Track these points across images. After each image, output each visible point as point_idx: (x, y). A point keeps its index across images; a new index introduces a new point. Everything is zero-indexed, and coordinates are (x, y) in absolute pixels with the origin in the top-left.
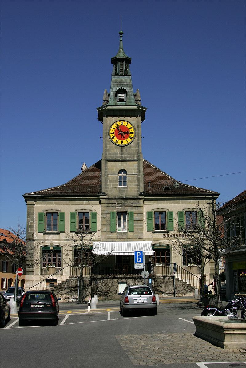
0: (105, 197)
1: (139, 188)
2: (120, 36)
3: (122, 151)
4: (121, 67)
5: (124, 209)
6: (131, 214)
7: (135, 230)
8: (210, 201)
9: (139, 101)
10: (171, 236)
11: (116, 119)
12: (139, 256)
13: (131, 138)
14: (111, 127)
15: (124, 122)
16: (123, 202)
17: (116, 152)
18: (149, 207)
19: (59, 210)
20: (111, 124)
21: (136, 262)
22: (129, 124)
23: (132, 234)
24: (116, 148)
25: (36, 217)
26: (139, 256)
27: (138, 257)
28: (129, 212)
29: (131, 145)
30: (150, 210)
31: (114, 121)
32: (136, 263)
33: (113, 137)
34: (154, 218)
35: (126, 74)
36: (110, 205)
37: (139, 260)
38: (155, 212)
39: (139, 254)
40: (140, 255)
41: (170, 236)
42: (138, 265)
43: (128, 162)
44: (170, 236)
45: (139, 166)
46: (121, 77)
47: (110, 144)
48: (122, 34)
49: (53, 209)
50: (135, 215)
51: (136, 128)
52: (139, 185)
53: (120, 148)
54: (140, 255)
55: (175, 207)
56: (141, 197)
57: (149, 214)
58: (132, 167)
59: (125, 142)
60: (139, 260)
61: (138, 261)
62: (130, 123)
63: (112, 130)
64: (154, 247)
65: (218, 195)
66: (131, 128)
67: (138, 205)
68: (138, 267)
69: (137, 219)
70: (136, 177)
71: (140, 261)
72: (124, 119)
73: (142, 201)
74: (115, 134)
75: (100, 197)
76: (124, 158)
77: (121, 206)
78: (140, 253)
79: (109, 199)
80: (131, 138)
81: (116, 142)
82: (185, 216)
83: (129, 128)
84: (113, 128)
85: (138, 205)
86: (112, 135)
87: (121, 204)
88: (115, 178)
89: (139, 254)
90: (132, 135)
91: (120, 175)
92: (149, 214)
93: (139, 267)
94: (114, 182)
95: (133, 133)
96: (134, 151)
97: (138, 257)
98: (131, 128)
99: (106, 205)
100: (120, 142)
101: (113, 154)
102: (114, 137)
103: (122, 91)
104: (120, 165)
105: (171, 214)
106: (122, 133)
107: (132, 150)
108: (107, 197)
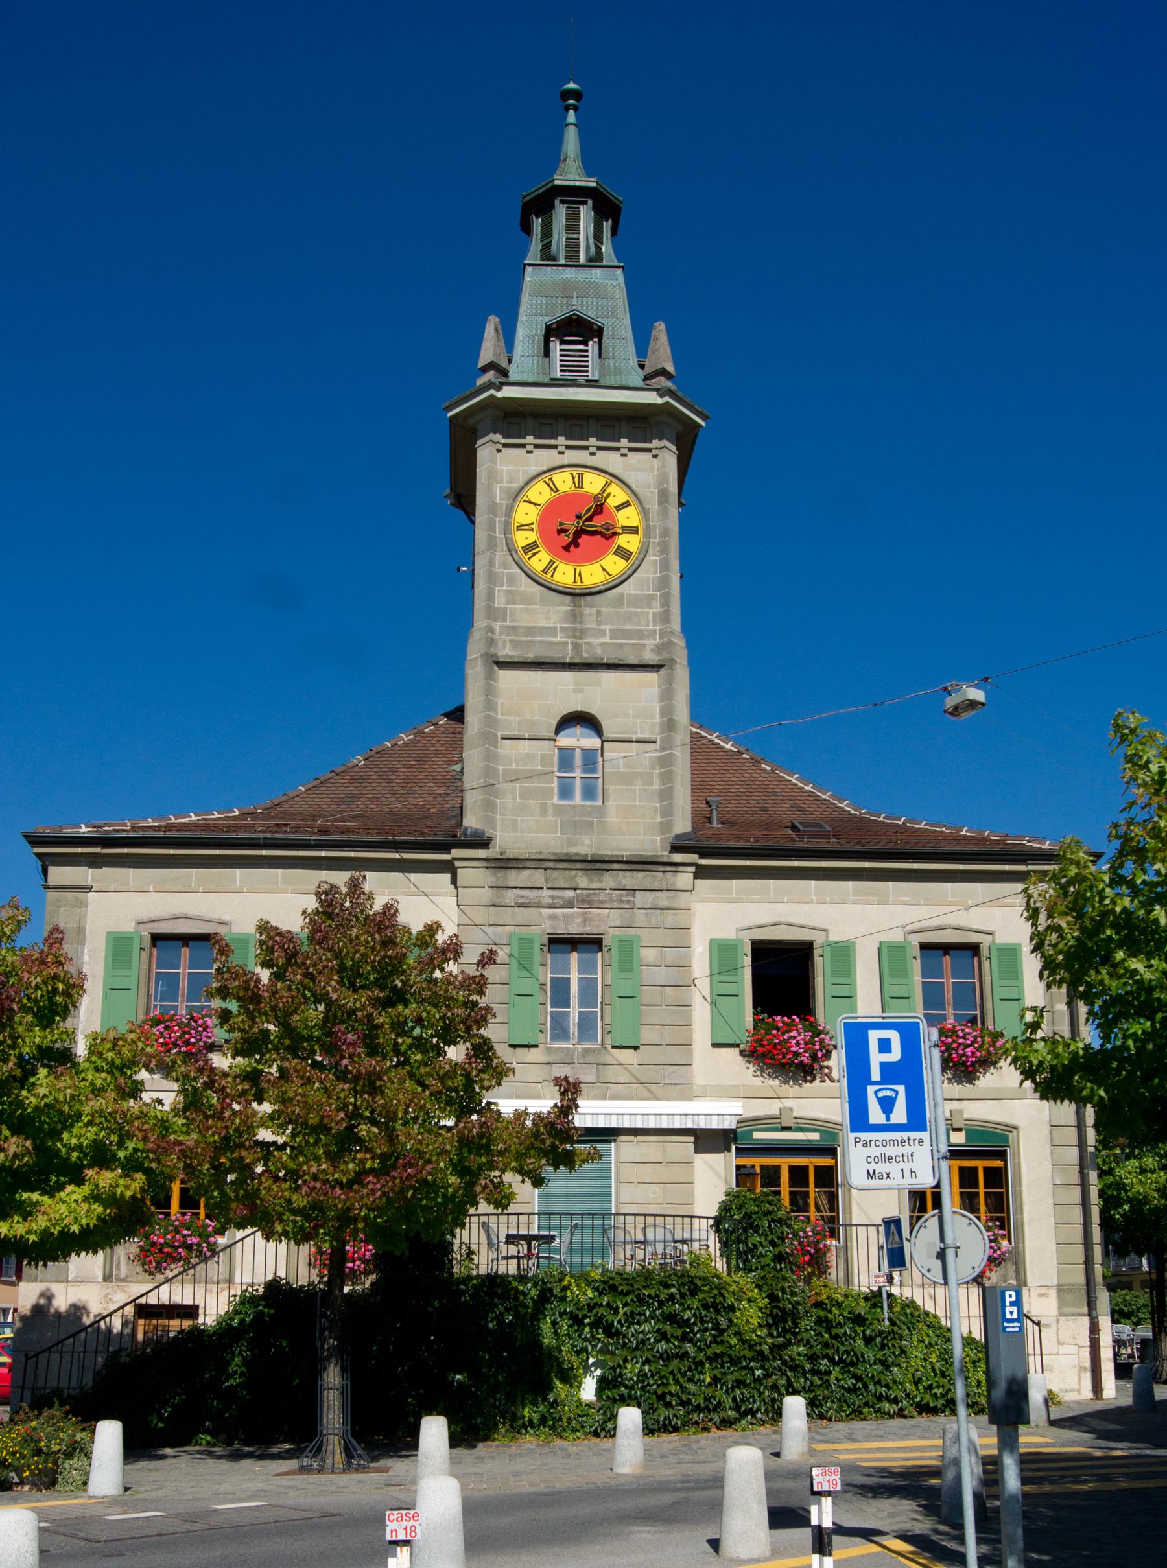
0: (481, 853)
1: (667, 812)
3: (575, 617)
4: (572, 226)
6: (628, 948)
11: (544, 458)
12: (884, 1066)
13: (623, 553)
14: (517, 495)
16: (582, 881)
17: (543, 623)
19: (226, 918)
20: (521, 482)
23: (626, 1056)
24: (544, 602)
25: (90, 957)
26: (884, 1066)
27: (876, 1075)
28: (611, 937)
29: (628, 589)
32: (865, 1136)
33: (531, 548)
36: (510, 896)
37: (887, 1105)
39: (885, 1046)
40: (895, 1055)
42: (873, 1151)
43: (607, 677)
45: (667, 695)
46: (570, 274)
47: (512, 580)
48: (577, 95)
50: (648, 955)
51: (653, 506)
52: (666, 795)
53: (564, 606)
54: (895, 1055)
56: (678, 857)
59: (592, 575)
60: (887, 1105)
61: (876, 1115)
63: (526, 514)
64: (751, 1132)
67: (663, 899)
68: (881, 1168)
69: (661, 975)
70: (651, 753)
71: (900, 1115)
73: (684, 879)
74: (542, 532)
75: (456, 853)
76: (586, 657)
77: (569, 905)
78: (894, 1036)
79: (503, 864)
80: (623, 553)
81: (545, 571)
82: (916, 967)
84: (530, 502)
85: (664, 903)
86: (522, 539)
87: (571, 894)
89: (885, 1046)
90: (630, 542)
95: (633, 530)
96: (643, 622)
97: (876, 1075)
99: (486, 895)
100: (564, 574)
101: (531, 631)
104: (564, 691)
105: (844, 952)
106: (582, 528)
107: (629, 618)
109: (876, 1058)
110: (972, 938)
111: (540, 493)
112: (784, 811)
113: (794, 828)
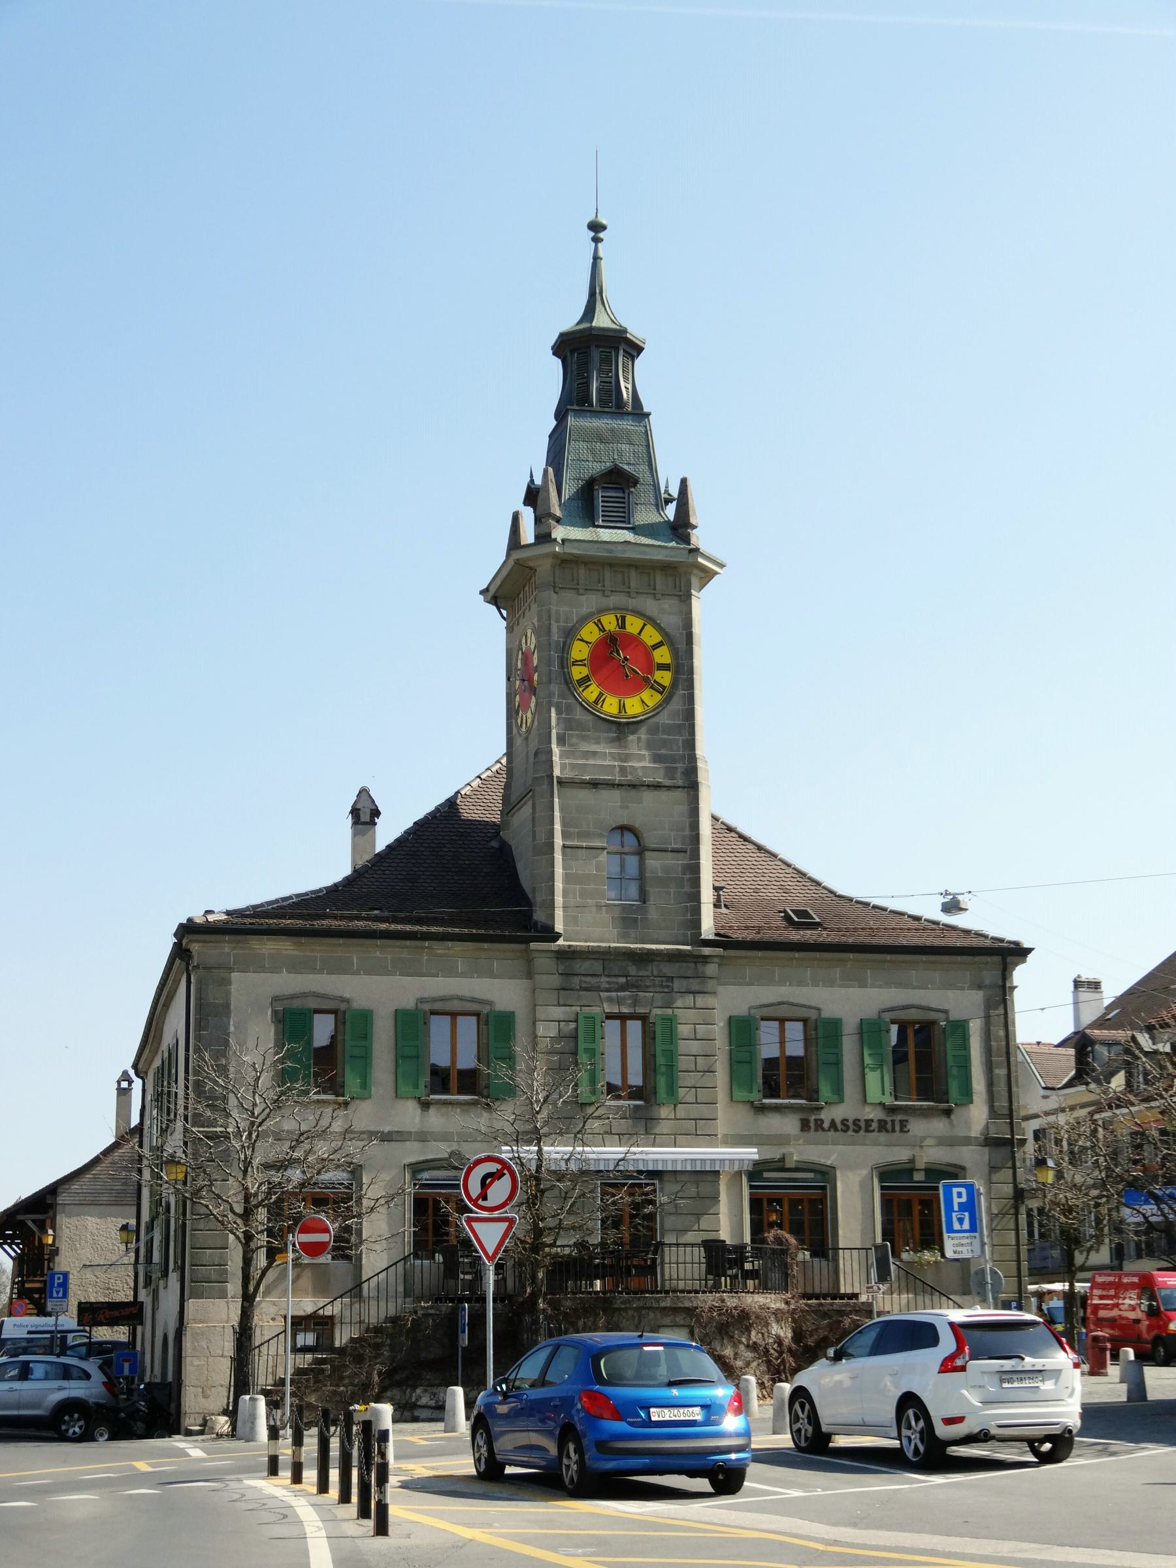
12: (959, 1204)
16: (632, 970)
19: (347, 995)
21: (950, 1230)
25: (236, 1028)
26: (959, 1204)
27: (956, 1208)
31: (585, 610)
32: (952, 1235)
33: (584, 681)
36: (576, 981)
40: (964, 1199)
41: (826, 1125)
42: (956, 1242)
44: (826, 1125)
50: (684, 1030)
54: (964, 1199)
61: (956, 1226)
64: (761, 1172)
68: (959, 1249)
69: (694, 1047)
71: (966, 1226)
72: (632, 603)
75: (533, 945)
77: (622, 988)
78: (963, 1190)
81: (596, 702)
84: (587, 643)
85: (696, 987)
86: (578, 673)
87: (623, 980)
89: (960, 1195)
90: (664, 678)
96: (675, 748)
97: (956, 1208)
100: (611, 706)
109: (956, 1201)
110: (932, 1016)
111: (590, 633)
112: (771, 893)
113: (787, 918)
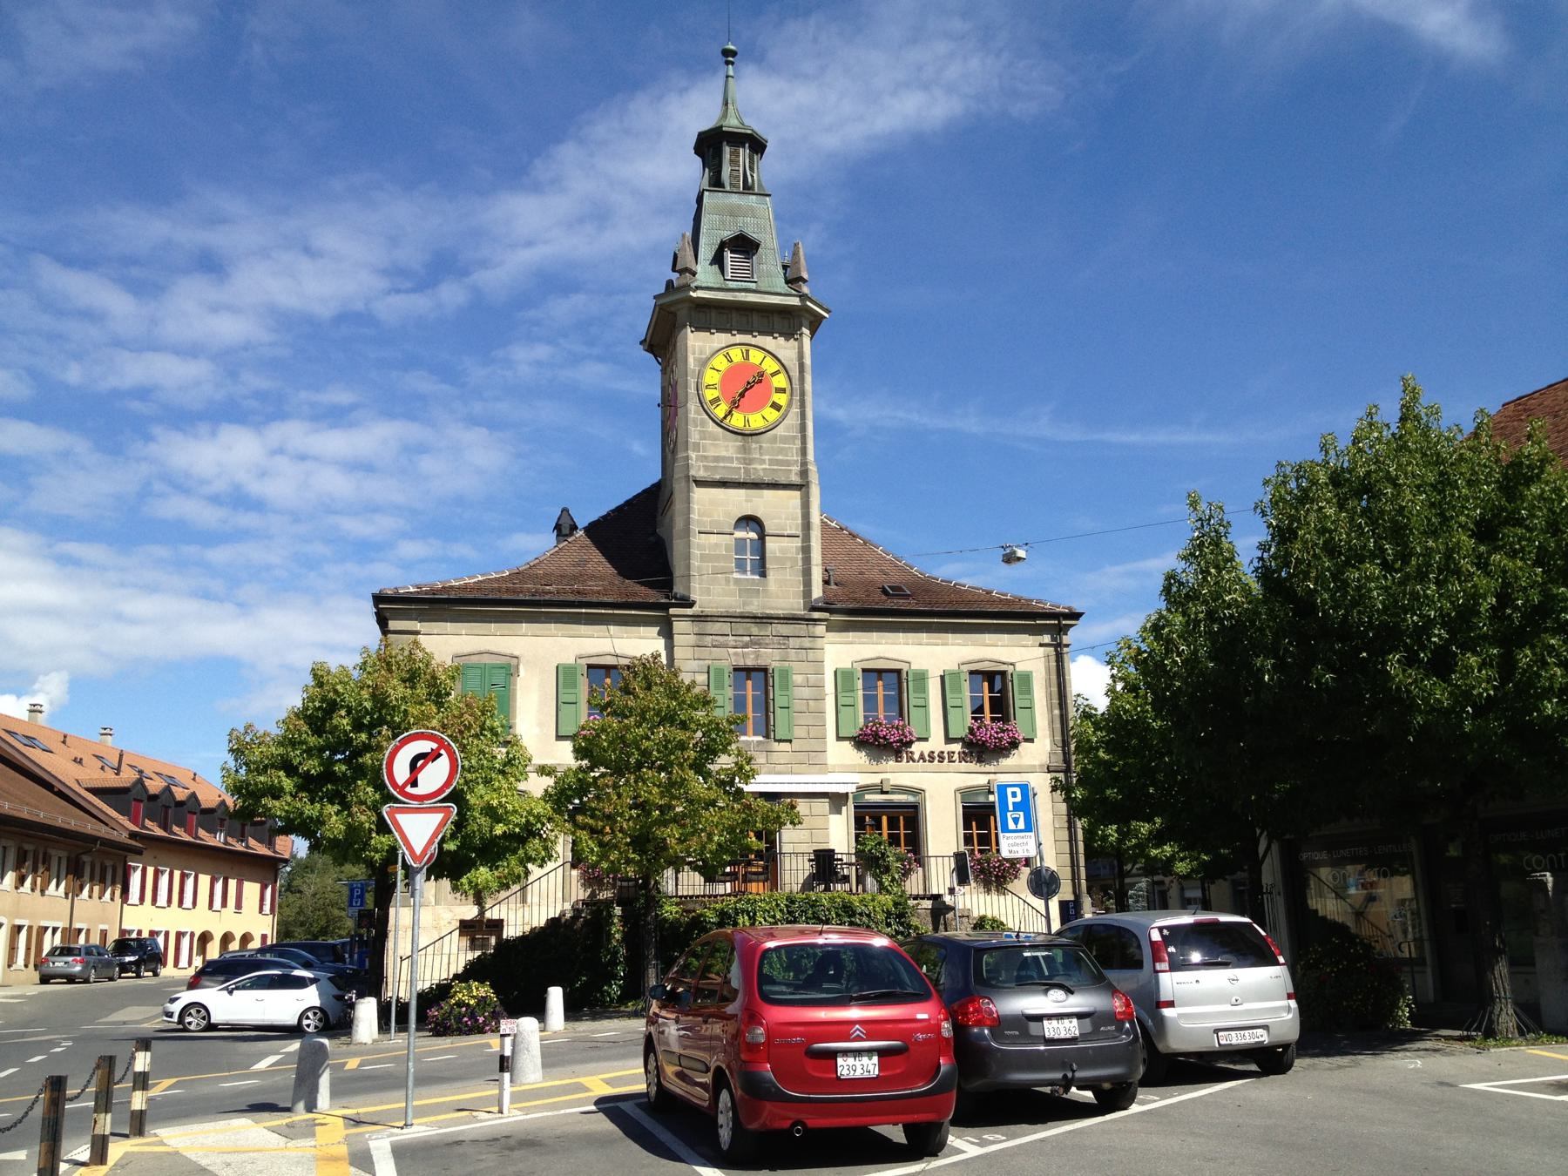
0: (689, 611)
1: (807, 584)
2: (727, 63)
3: (745, 449)
4: (734, 162)
5: (757, 657)
6: (785, 674)
7: (799, 732)
8: (1047, 639)
9: (805, 281)
10: (922, 757)
11: (722, 339)
13: (776, 407)
14: (704, 363)
15: (753, 352)
16: (755, 630)
17: (724, 454)
18: (845, 651)
20: (708, 353)
21: (1006, 829)
22: (769, 360)
23: (785, 746)
24: (725, 439)
28: (773, 664)
29: (780, 431)
30: (846, 664)
31: (717, 346)
33: (715, 401)
34: (860, 693)
35: (748, 189)
37: (1016, 821)
38: (864, 670)
39: (1014, 794)
40: (1018, 799)
41: (916, 757)
43: (767, 493)
44: (916, 757)
45: (806, 505)
46: (735, 199)
47: (703, 423)
48: (734, 54)
49: (494, 649)
50: (798, 679)
51: (795, 374)
52: (807, 573)
53: (737, 442)
54: (1018, 799)
55: (933, 656)
56: (816, 615)
57: (843, 678)
58: (778, 508)
59: (756, 421)
60: (1016, 821)
61: (1011, 826)
62: (773, 354)
63: (711, 377)
65: (1076, 616)
66: (777, 373)
67: (806, 642)
69: (806, 692)
70: (798, 543)
71: (1021, 825)
72: (753, 341)
73: (820, 629)
74: (723, 392)
75: (672, 611)
76: (753, 478)
77: (746, 646)
78: (1018, 790)
79: (700, 618)
80: (776, 407)
82: (966, 686)
83: (770, 371)
85: (808, 645)
86: (710, 395)
88: (721, 544)
89: (1014, 794)
90: (782, 399)
91: (740, 534)
92: (843, 678)
93: (1019, 849)
94: (717, 558)
95: (783, 391)
98: (777, 373)
99: (692, 639)
100: (737, 420)
101: (717, 459)
102: (717, 400)
103: (744, 245)
104: (739, 502)
105: (922, 677)
106: (747, 388)
107: (781, 451)
108: (695, 610)
109: (1011, 800)
110: (1003, 668)
111: (720, 362)
112: (874, 575)
113: (884, 592)
